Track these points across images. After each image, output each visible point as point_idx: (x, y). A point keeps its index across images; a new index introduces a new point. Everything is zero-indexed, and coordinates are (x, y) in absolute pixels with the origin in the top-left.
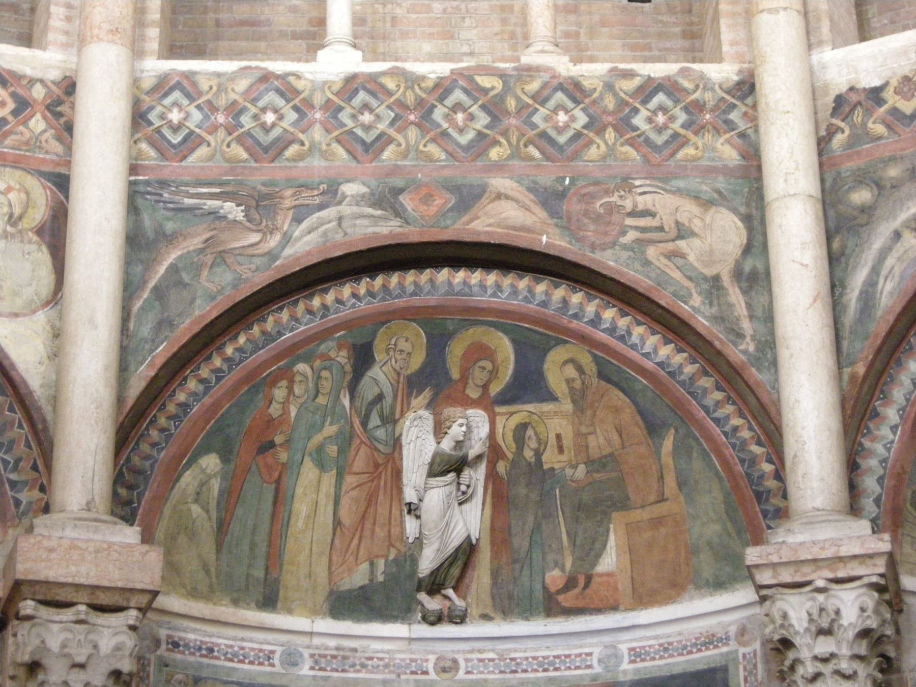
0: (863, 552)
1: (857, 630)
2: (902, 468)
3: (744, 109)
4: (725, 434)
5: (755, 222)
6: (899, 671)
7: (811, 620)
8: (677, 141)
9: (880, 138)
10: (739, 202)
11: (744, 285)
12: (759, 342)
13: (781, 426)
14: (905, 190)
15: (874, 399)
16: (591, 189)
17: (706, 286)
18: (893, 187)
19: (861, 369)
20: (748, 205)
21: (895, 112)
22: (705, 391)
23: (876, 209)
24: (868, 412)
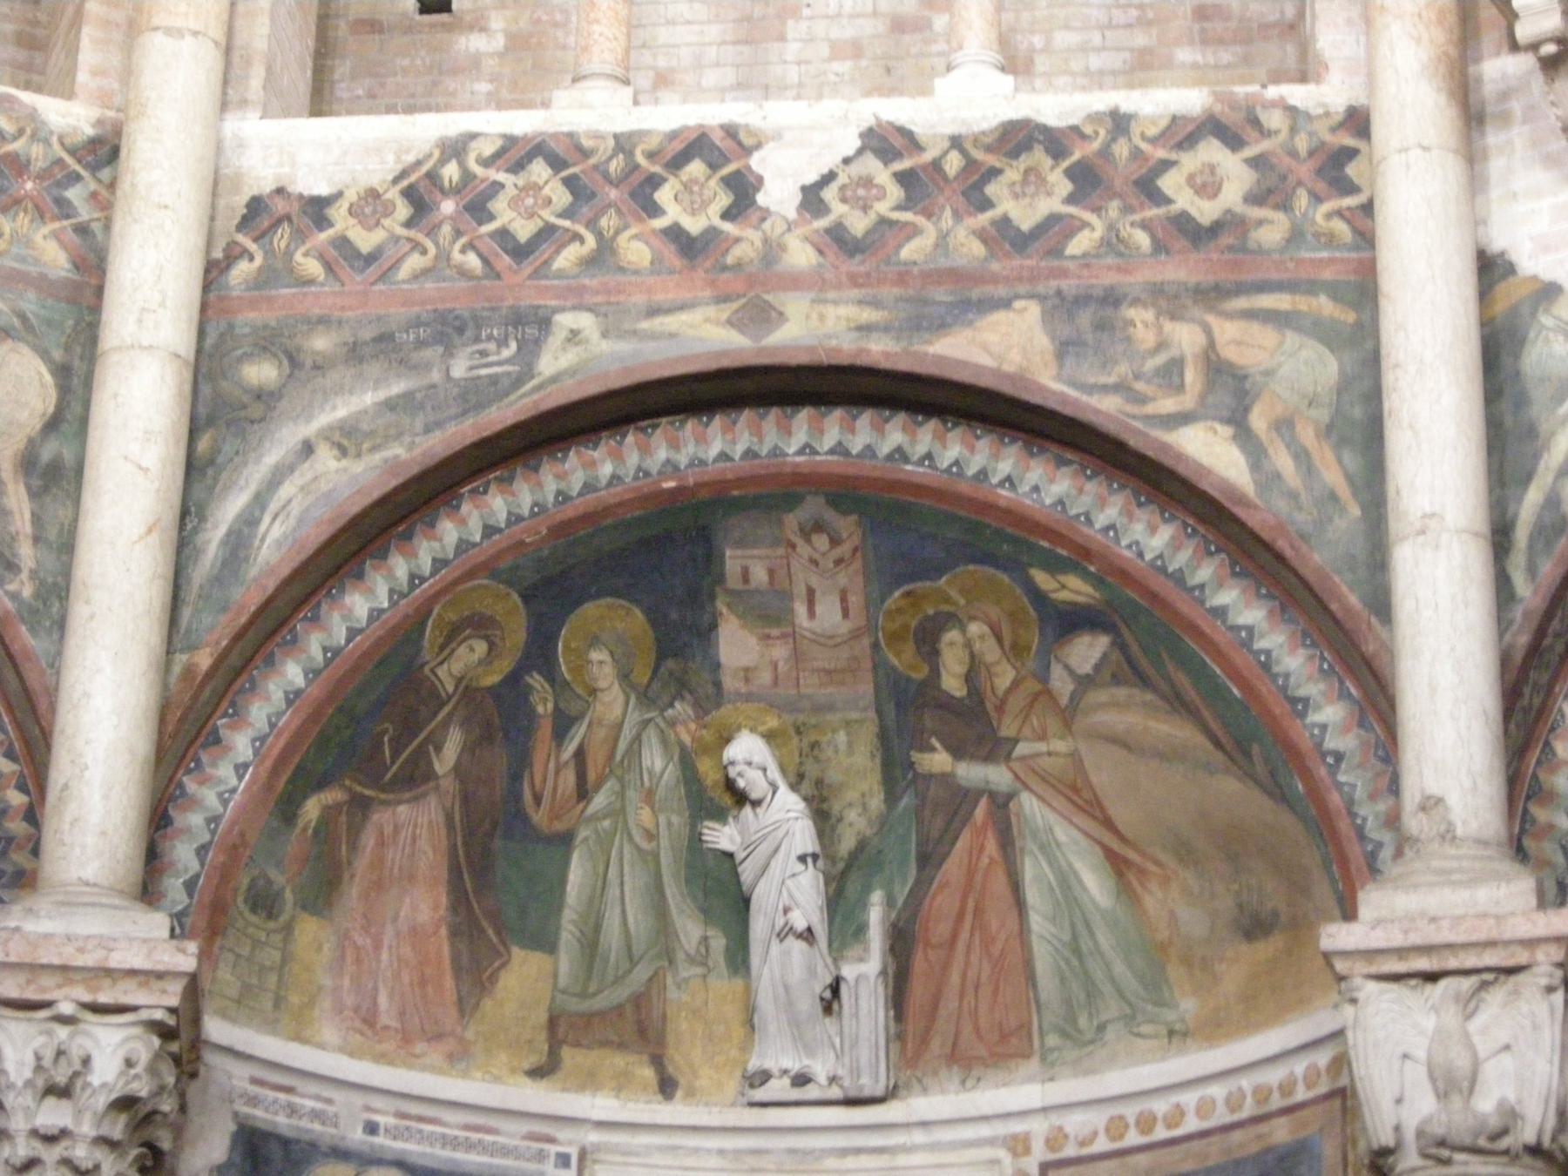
0: (147, 966)
1: (114, 1096)
2: (242, 835)
3: (93, 186)
5: (75, 380)
7: (39, 1068)
9: (311, 282)
11: (37, 483)
12: (42, 583)
13: (51, 732)
14: (333, 377)
15: (218, 714)
18: (316, 367)
19: (204, 660)
20: (67, 349)
21: (343, 243)
23: (281, 397)
24: (205, 732)
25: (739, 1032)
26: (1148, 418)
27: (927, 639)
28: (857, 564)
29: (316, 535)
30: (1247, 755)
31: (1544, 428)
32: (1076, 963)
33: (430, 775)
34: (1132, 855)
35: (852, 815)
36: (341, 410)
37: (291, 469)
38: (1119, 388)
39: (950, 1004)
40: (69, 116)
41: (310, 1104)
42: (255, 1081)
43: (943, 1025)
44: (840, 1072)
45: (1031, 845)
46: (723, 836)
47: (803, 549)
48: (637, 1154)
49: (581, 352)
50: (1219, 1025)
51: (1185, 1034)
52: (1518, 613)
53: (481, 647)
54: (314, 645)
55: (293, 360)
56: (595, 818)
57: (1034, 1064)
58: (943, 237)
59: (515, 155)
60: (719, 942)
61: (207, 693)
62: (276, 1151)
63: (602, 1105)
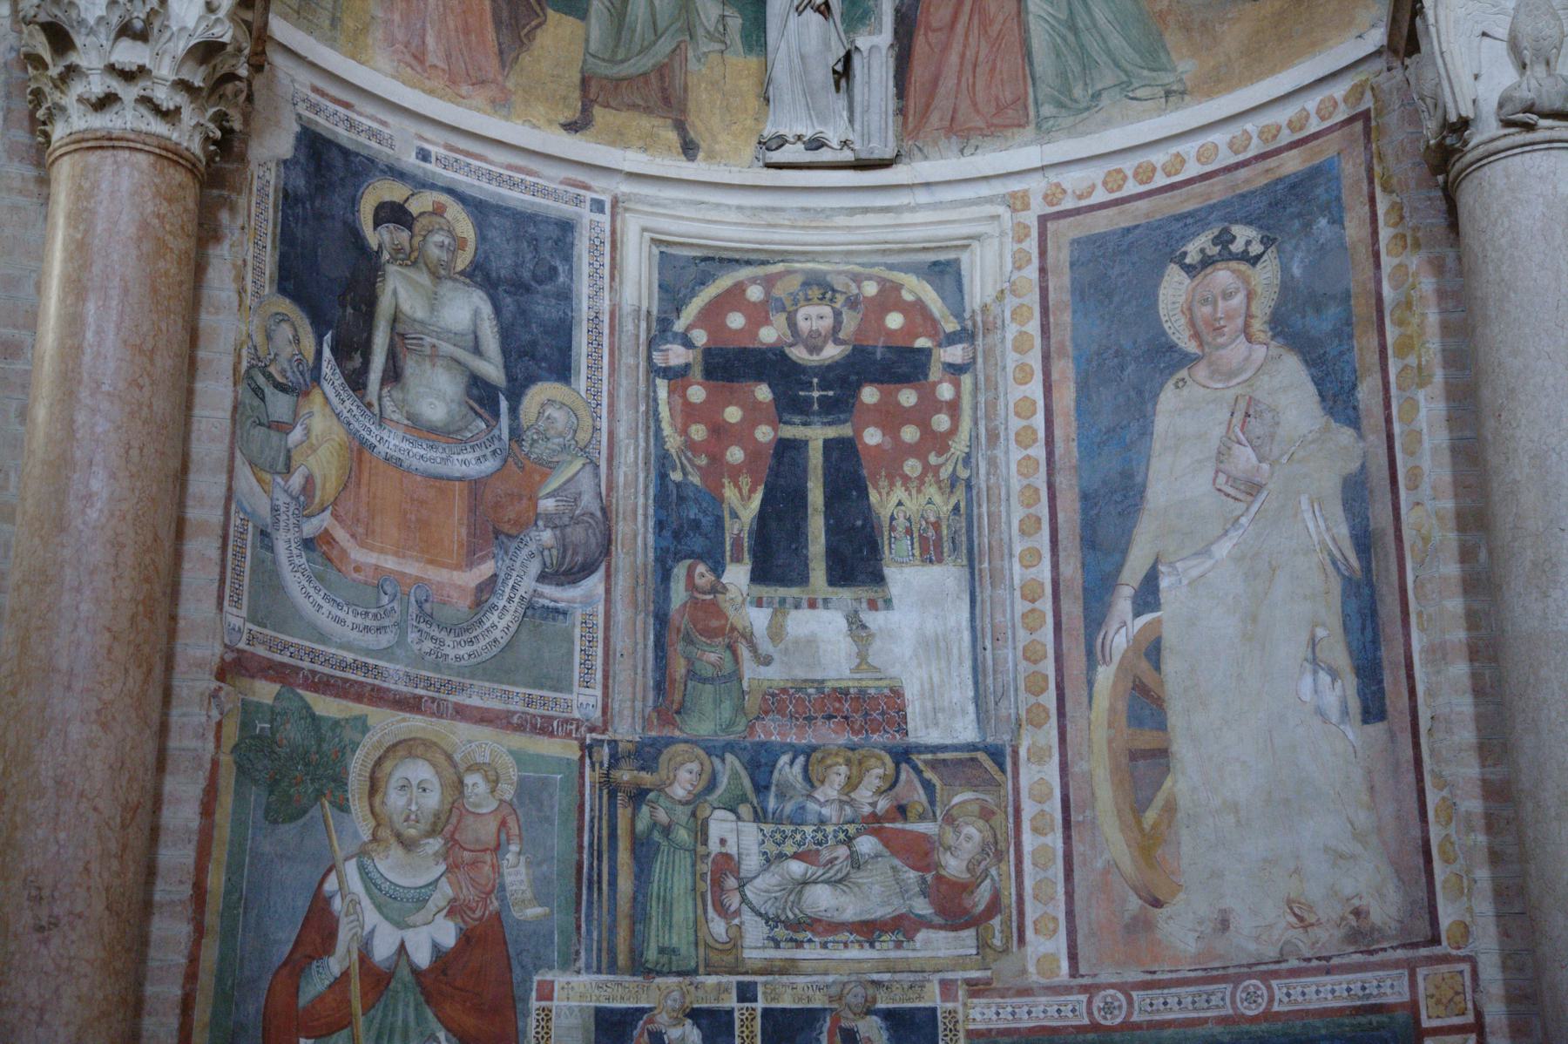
6: (242, 158)
25: (754, 103)
32: (1071, 38)
39: (948, 83)
42: (316, 90)
44: (851, 137)
48: (664, 206)
50: (1219, 81)
51: (1183, 93)
57: (1030, 131)
60: (735, 22)
63: (633, 160)
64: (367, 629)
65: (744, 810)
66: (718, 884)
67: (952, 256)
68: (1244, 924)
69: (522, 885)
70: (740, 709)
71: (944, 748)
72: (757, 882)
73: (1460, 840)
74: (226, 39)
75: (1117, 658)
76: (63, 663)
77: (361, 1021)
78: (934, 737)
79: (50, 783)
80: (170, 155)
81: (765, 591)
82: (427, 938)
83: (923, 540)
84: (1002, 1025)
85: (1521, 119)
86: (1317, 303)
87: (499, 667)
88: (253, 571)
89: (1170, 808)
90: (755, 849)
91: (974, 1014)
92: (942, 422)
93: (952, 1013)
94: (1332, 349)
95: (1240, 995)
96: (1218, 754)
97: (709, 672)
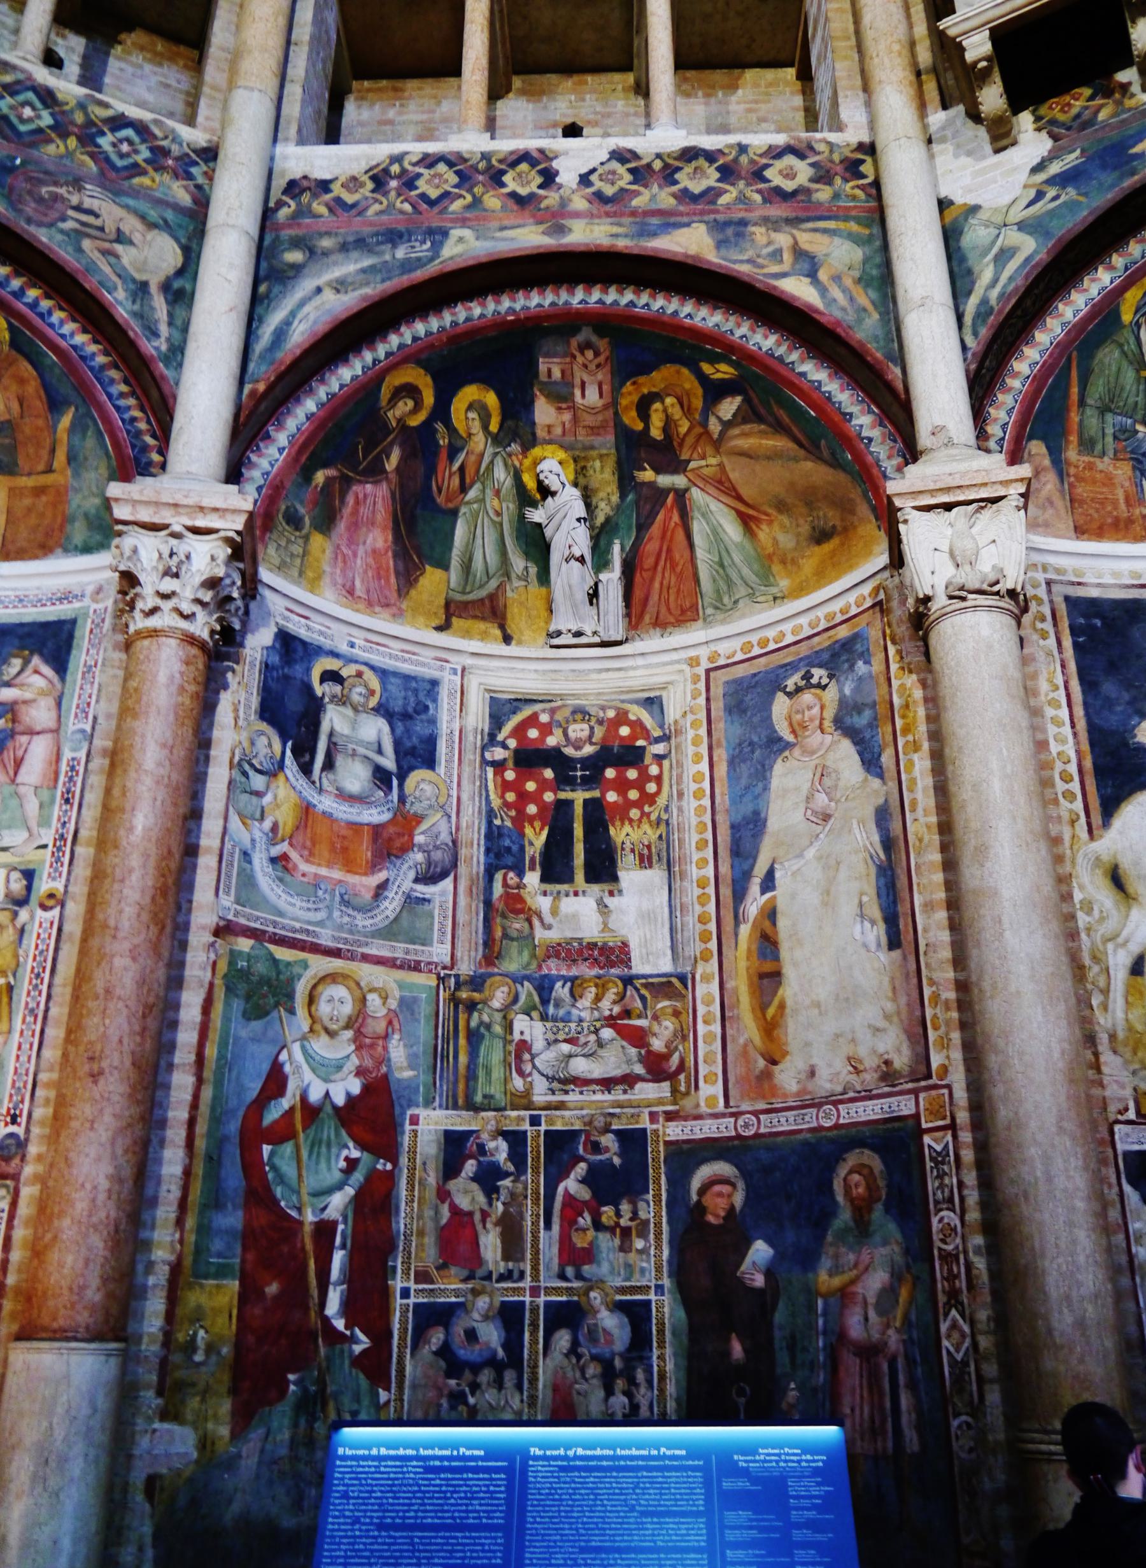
1: (204, 578)
3: (205, 168)
4: (123, 420)
8: (136, 170)
9: (321, 216)
10: (181, 234)
11: (170, 297)
14: (333, 258)
16: (41, 176)
17: (132, 286)
19: (261, 387)
20: (189, 239)
21: (338, 200)
22: (112, 381)
25: (544, 614)
26: (764, 275)
27: (643, 408)
28: (608, 368)
29: (322, 328)
30: (818, 447)
31: (976, 269)
33: (384, 471)
34: (751, 512)
35: (602, 505)
36: (337, 273)
37: (310, 299)
38: (749, 261)
39: (654, 597)
40: (195, 136)
41: (318, 627)
43: (651, 609)
45: (696, 514)
46: (536, 516)
47: (580, 359)
49: (463, 246)
52: (969, 355)
53: (410, 404)
54: (322, 393)
55: (312, 251)
56: (468, 503)
57: (700, 623)
58: (653, 198)
59: (428, 161)
60: (533, 570)
61: (262, 407)
62: (300, 648)
63: (475, 646)
64: (309, 909)
65: (535, 1014)
66: (518, 1057)
67: (657, 693)
68: (823, 1073)
69: (402, 1060)
70: (533, 956)
71: (651, 976)
72: (542, 1056)
73: (942, 1017)
74: (221, 575)
75: (751, 920)
76: (112, 923)
77: (301, 1136)
78: (647, 970)
79: (101, 991)
80: (190, 640)
81: (549, 887)
82: (346, 1087)
83: (641, 856)
84: (685, 1137)
85: (958, 594)
86: (858, 708)
87: (389, 932)
88: (238, 874)
89: (782, 1006)
90: (541, 1037)
91: (668, 1131)
92: (651, 787)
93: (656, 1131)
94: (868, 735)
95: (821, 1114)
96: (806, 975)
97: (515, 934)
